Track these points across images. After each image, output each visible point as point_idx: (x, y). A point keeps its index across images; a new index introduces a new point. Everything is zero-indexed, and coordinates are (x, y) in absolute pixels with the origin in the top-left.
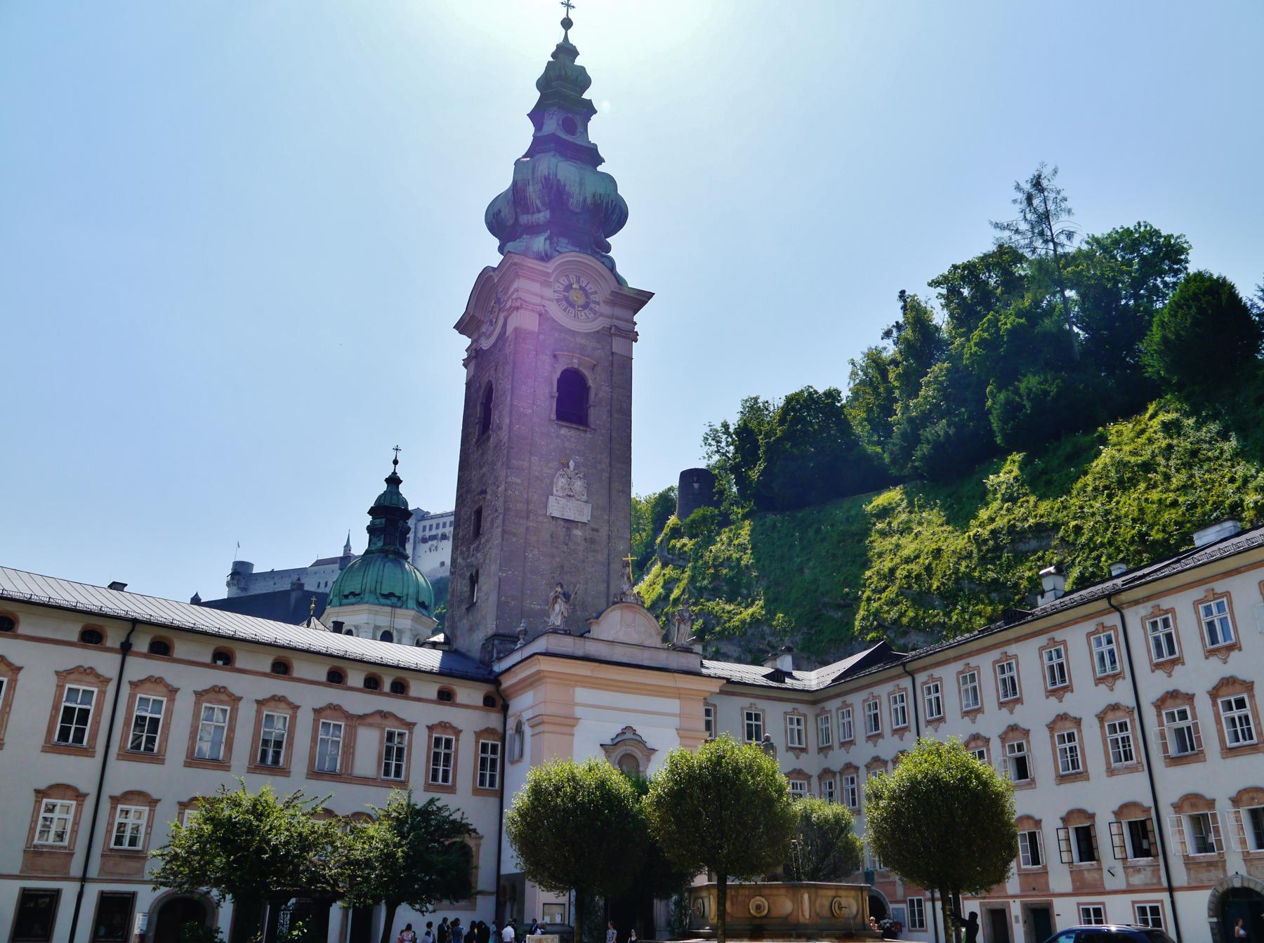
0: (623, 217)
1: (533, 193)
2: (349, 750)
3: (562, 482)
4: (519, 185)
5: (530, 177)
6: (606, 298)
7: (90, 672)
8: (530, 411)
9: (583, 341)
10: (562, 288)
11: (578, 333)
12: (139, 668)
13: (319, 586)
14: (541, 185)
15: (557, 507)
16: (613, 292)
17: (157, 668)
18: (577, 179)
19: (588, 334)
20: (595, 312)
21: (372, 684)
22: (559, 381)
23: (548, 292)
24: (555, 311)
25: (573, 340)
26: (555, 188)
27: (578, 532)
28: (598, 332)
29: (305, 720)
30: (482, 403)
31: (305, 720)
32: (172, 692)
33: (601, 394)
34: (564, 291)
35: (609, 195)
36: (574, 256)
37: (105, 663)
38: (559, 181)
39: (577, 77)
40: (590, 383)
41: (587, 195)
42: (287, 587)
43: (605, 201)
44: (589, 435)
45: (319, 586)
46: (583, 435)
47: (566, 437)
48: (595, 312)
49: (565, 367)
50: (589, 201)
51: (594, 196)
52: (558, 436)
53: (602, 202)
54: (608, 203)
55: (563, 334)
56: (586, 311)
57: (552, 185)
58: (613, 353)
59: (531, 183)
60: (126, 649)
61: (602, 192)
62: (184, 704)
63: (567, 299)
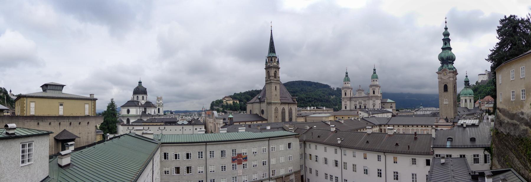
1: (440, 59)
2: (424, 132)
3: (445, 100)
7: (404, 129)
12: (407, 128)
15: (445, 103)
17: (408, 128)
21: (425, 126)
22: (444, 87)
23: (442, 75)
24: (443, 77)
27: (447, 105)
29: (420, 130)
31: (420, 130)
32: (410, 130)
37: (405, 128)
44: (448, 93)
60: (406, 127)
62: (410, 130)
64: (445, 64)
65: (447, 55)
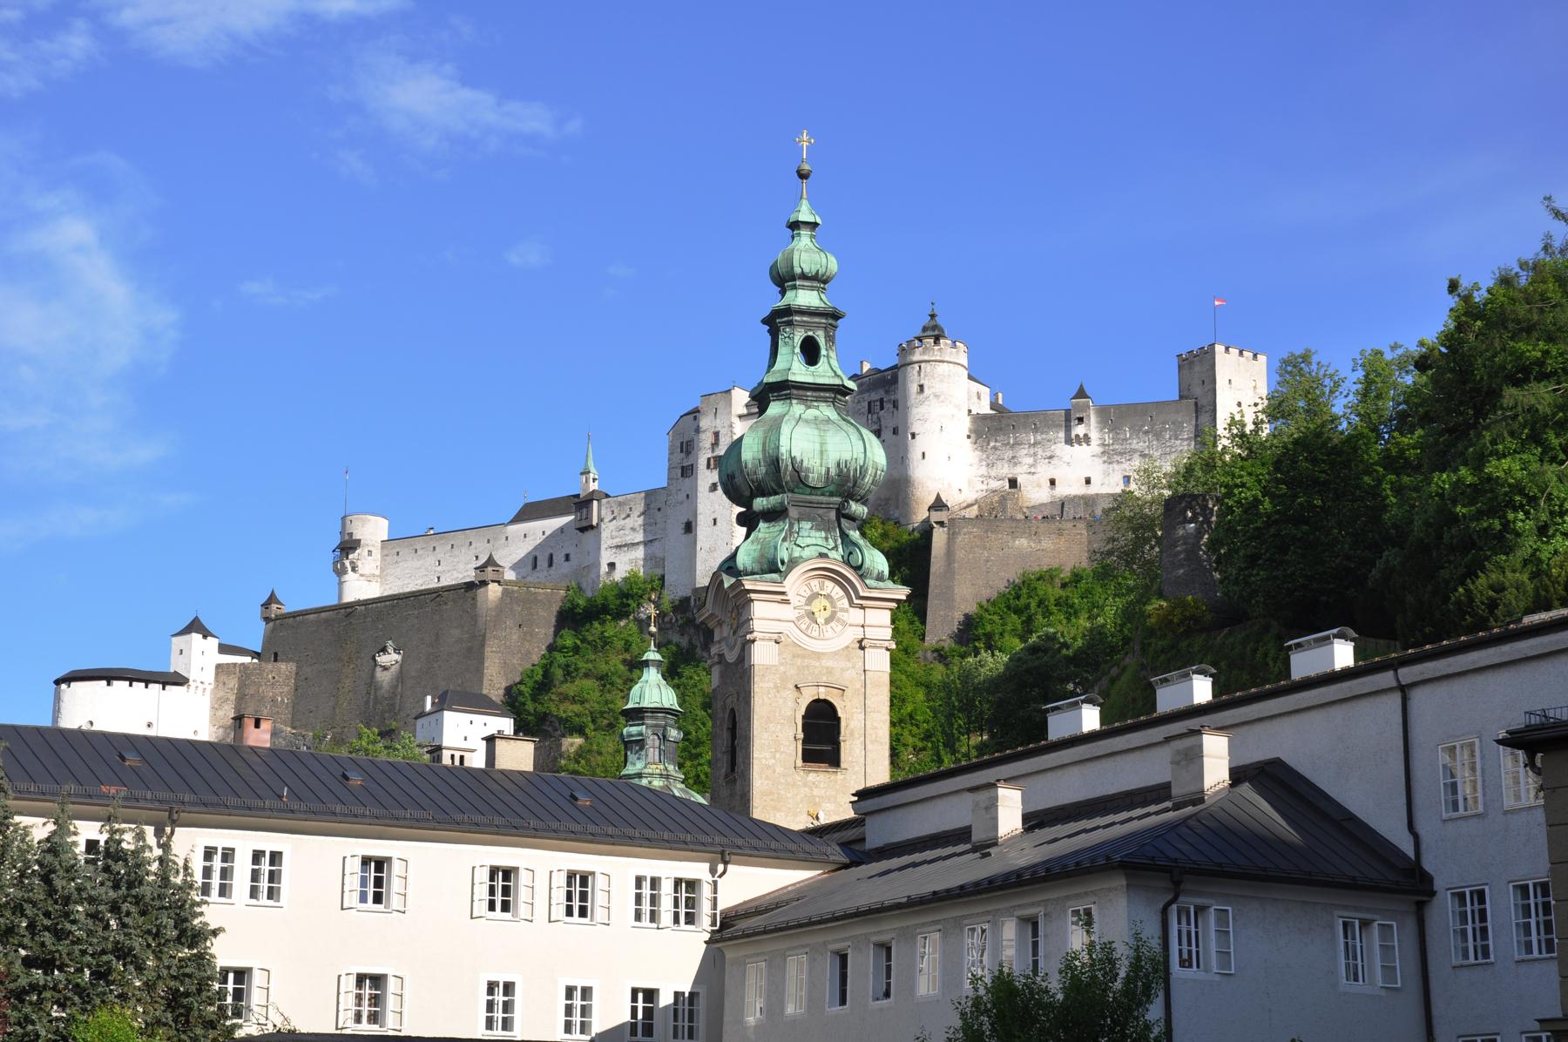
0: (879, 472)
5: (761, 457)
8: (773, 761)
10: (803, 600)
11: (823, 654)
13: (535, 567)
18: (817, 447)
19: (836, 653)
20: (844, 624)
25: (818, 664)
26: (790, 468)
28: (847, 647)
30: (728, 729)
33: (853, 724)
34: (806, 604)
35: (856, 459)
36: (812, 564)
38: (793, 459)
40: (840, 714)
42: (469, 575)
43: (852, 469)
44: (840, 776)
45: (535, 567)
46: (833, 777)
47: (814, 784)
48: (844, 624)
49: (811, 700)
50: (833, 472)
51: (839, 464)
52: (805, 785)
53: (848, 470)
55: (806, 661)
56: (833, 624)
61: (849, 458)
64: (806, 525)
65: (846, 456)
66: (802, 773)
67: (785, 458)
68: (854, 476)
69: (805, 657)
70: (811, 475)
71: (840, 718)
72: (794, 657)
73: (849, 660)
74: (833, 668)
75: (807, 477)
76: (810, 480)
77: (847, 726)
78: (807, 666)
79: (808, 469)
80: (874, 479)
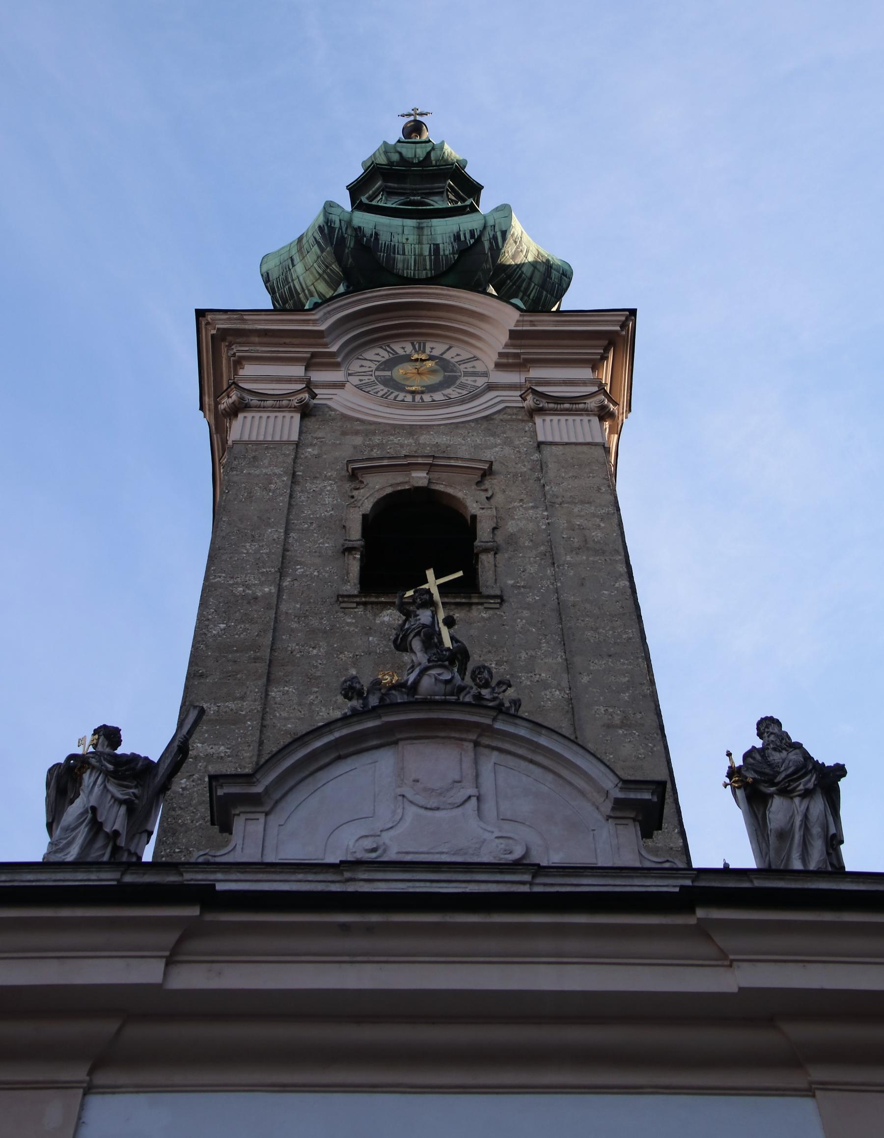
4: (273, 276)
6: (501, 355)
9: (443, 440)
14: (316, 248)
16: (513, 334)
26: (350, 243)
33: (511, 526)
34: (377, 369)
39: (429, 154)
41: (439, 241)
50: (447, 249)
53: (478, 241)
54: (495, 238)
57: (342, 240)
58: (540, 445)
59: (297, 259)
63: (388, 382)
66: (360, 610)
67: (337, 225)
68: (491, 248)
69: (374, 434)
70: (399, 257)
71: (474, 517)
72: (344, 433)
73: (494, 435)
74: (449, 446)
75: (391, 261)
76: (400, 266)
77: (494, 529)
78: (381, 446)
79: (391, 249)
80: (545, 281)
